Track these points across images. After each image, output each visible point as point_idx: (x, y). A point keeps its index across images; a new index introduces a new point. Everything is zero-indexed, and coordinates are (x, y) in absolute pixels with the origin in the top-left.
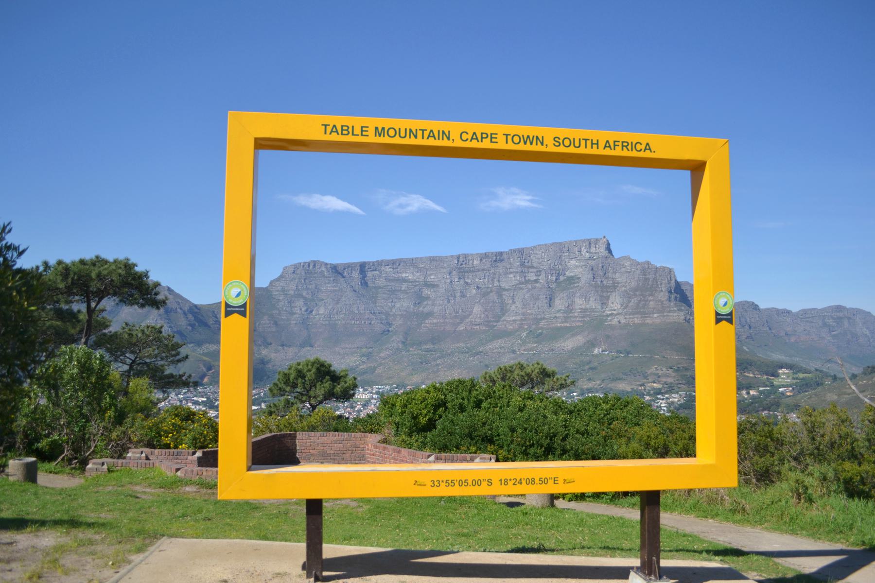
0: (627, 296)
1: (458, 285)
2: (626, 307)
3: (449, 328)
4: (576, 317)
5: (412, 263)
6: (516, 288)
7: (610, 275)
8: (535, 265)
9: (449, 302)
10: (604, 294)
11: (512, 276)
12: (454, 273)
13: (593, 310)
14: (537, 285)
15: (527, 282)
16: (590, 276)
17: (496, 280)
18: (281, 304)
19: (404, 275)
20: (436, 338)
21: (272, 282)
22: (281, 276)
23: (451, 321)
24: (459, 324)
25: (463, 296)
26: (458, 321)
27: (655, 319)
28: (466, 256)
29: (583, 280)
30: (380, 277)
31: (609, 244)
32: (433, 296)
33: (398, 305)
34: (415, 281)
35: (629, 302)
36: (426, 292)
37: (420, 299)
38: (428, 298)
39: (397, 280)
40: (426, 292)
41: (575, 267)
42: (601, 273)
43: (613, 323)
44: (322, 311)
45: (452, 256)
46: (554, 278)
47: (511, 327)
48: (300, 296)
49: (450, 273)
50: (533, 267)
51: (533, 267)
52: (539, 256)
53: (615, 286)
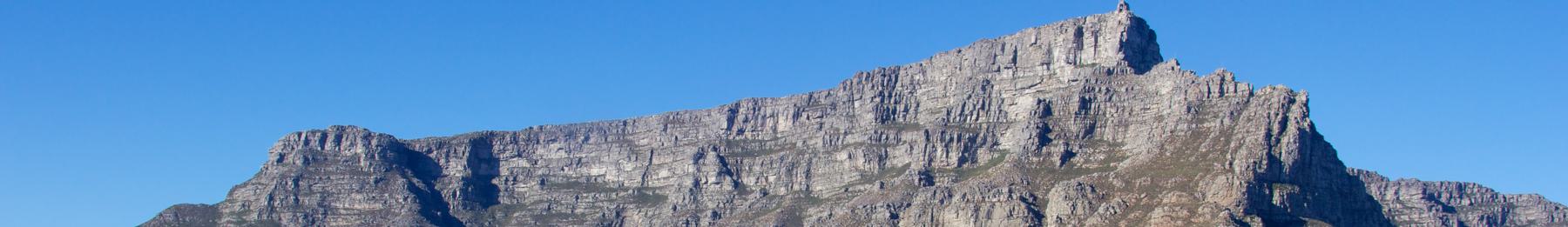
1: (715, 189)
7: (1108, 135)
11: (843, 156)
12: (711, 156)
17: (800, 177)
30: (529, 174)
39: (571, 185)
42: (1074, 127)
46: (954, 157)
49: (699, 157)
52: (939, 89)
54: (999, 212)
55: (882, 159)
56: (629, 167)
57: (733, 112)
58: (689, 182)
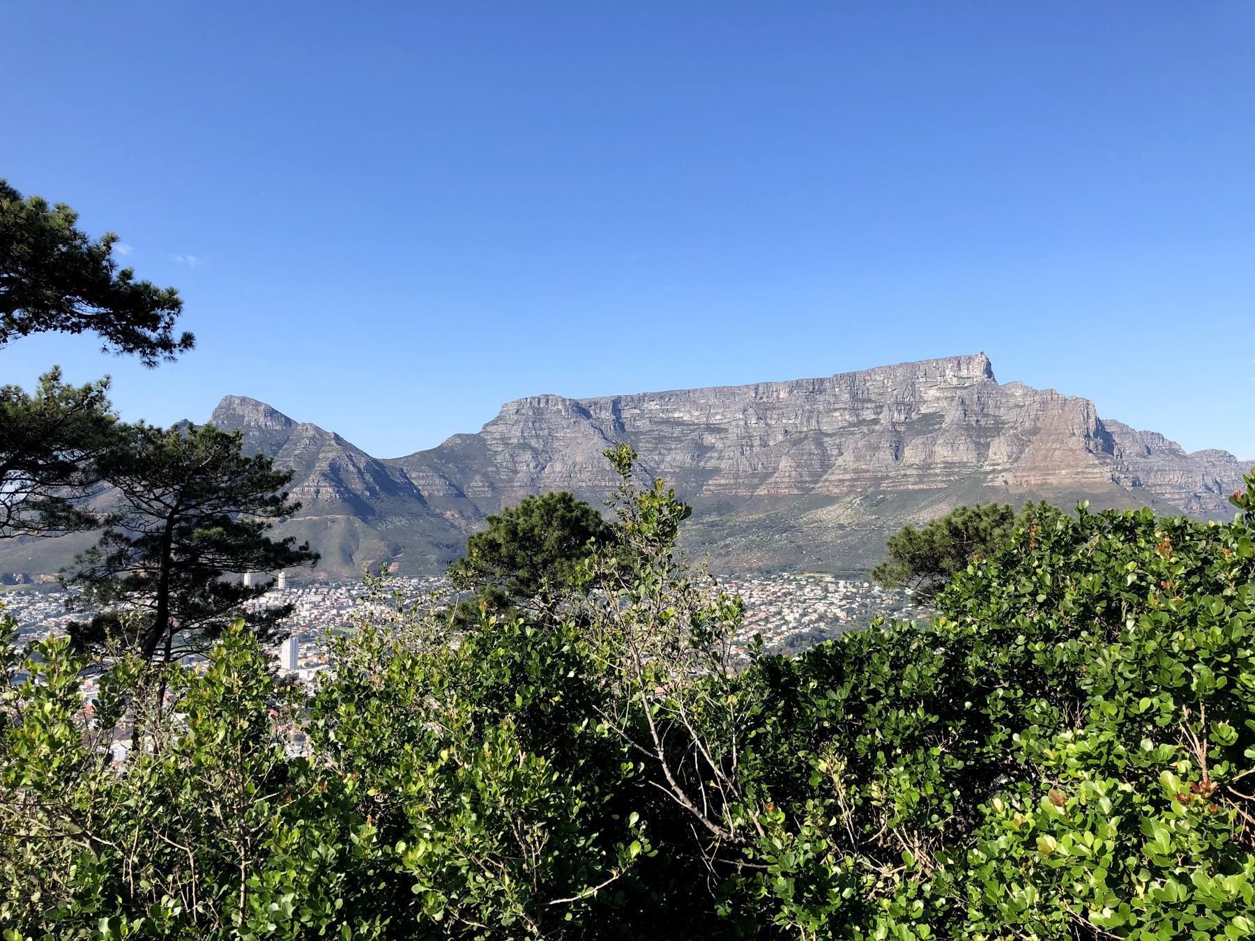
0: (1021, 442)
2: (1016, 460)
3: (742, 492)
4: (937, 475)
5: (685, 397)
6: (843, 432)
8: (873, 397)
9: (742, 453)
10: (982, 441)
11: (837, 414)
12: (751, 411)
13: (964, 465)
14: (877, 427)
15: (861, 422)
16: (959, 413)
17: (813, 422)
18: (499, 459)
19: (676, 415)
20: (724, 506)
21: (487, 425)
22: (500, 418)
23: (746, 481)
24: (756, 486)
25: (764, 445)
26: (756, 481)
27: (1063, 477)
28: (768, 385)
29: (947, 420)
30: (641, 416)
31: (989, 364)
32: (719, 445)
33: (668, 458)
34: (694, 424)
35: (1021, 452)
36: (710, 439)
37: (701, 450)
38: (712, 448)
39: (666, 422)
40: (710, 439)
41: (932, 398)
43: (996, 484)
44: (558, 467)
45: (747, 386)
46: (903, 417)
47: (836, 491)
48: (525, 446)
50: (870, 401)
51: (870, 401)
53: (998, 427)
54: (961, 447)
55: (857, 416)
56: (697, 413)
57: (757, 388)
58: (742, 423)
